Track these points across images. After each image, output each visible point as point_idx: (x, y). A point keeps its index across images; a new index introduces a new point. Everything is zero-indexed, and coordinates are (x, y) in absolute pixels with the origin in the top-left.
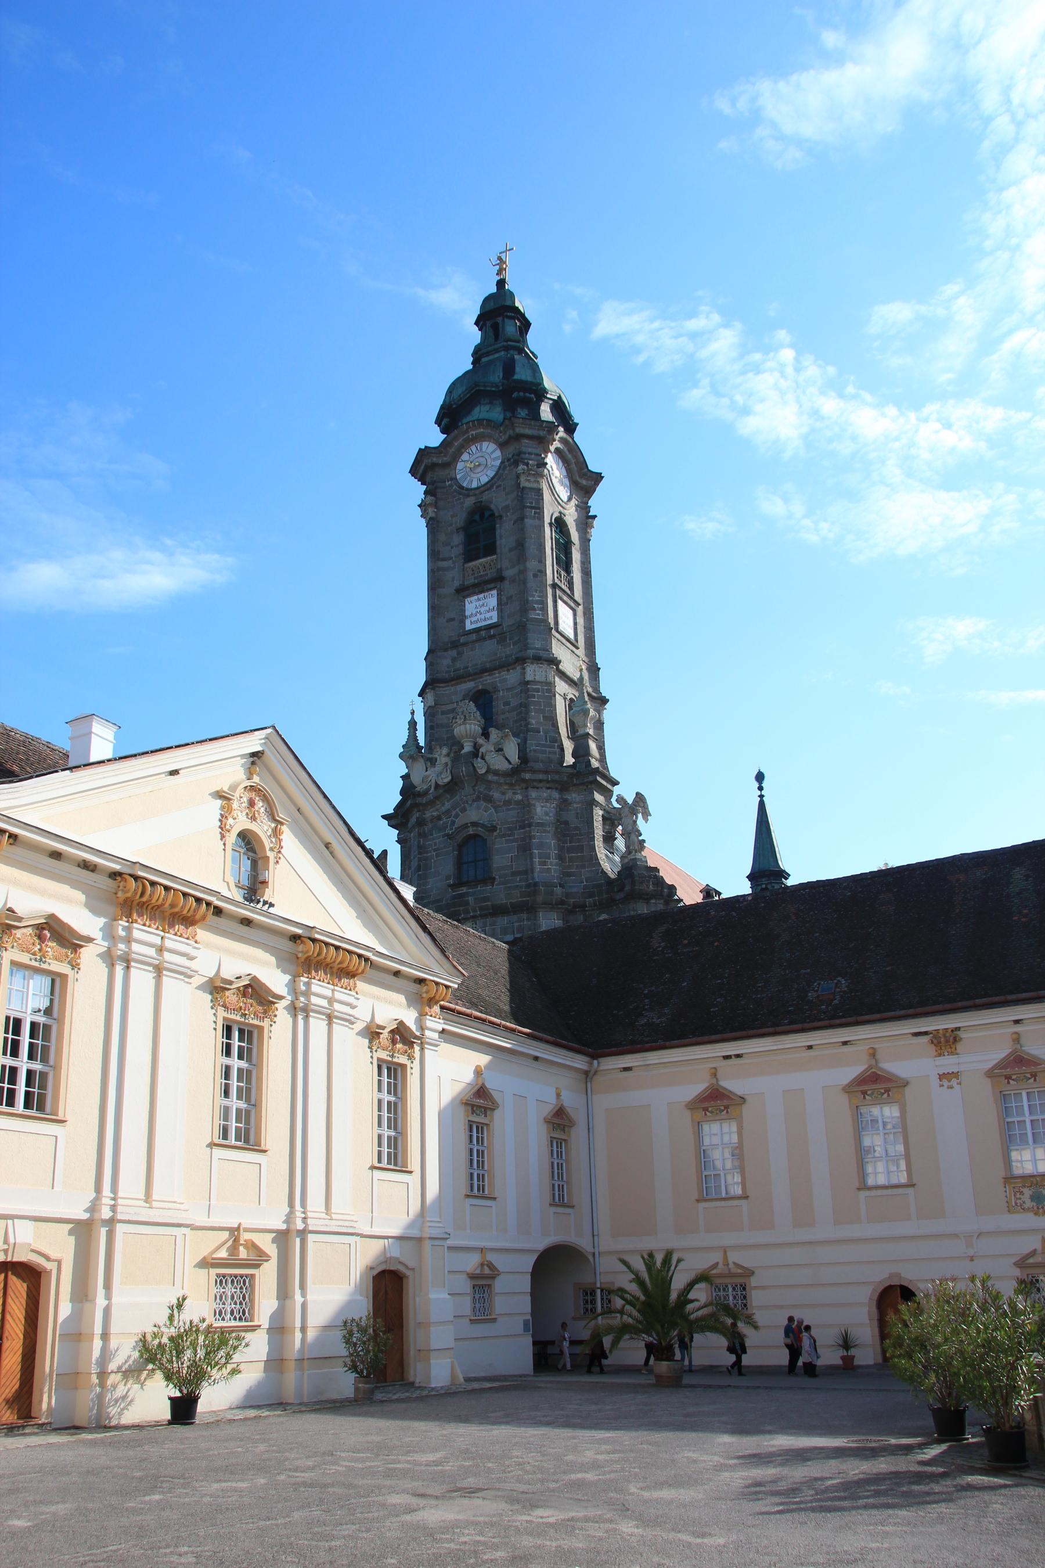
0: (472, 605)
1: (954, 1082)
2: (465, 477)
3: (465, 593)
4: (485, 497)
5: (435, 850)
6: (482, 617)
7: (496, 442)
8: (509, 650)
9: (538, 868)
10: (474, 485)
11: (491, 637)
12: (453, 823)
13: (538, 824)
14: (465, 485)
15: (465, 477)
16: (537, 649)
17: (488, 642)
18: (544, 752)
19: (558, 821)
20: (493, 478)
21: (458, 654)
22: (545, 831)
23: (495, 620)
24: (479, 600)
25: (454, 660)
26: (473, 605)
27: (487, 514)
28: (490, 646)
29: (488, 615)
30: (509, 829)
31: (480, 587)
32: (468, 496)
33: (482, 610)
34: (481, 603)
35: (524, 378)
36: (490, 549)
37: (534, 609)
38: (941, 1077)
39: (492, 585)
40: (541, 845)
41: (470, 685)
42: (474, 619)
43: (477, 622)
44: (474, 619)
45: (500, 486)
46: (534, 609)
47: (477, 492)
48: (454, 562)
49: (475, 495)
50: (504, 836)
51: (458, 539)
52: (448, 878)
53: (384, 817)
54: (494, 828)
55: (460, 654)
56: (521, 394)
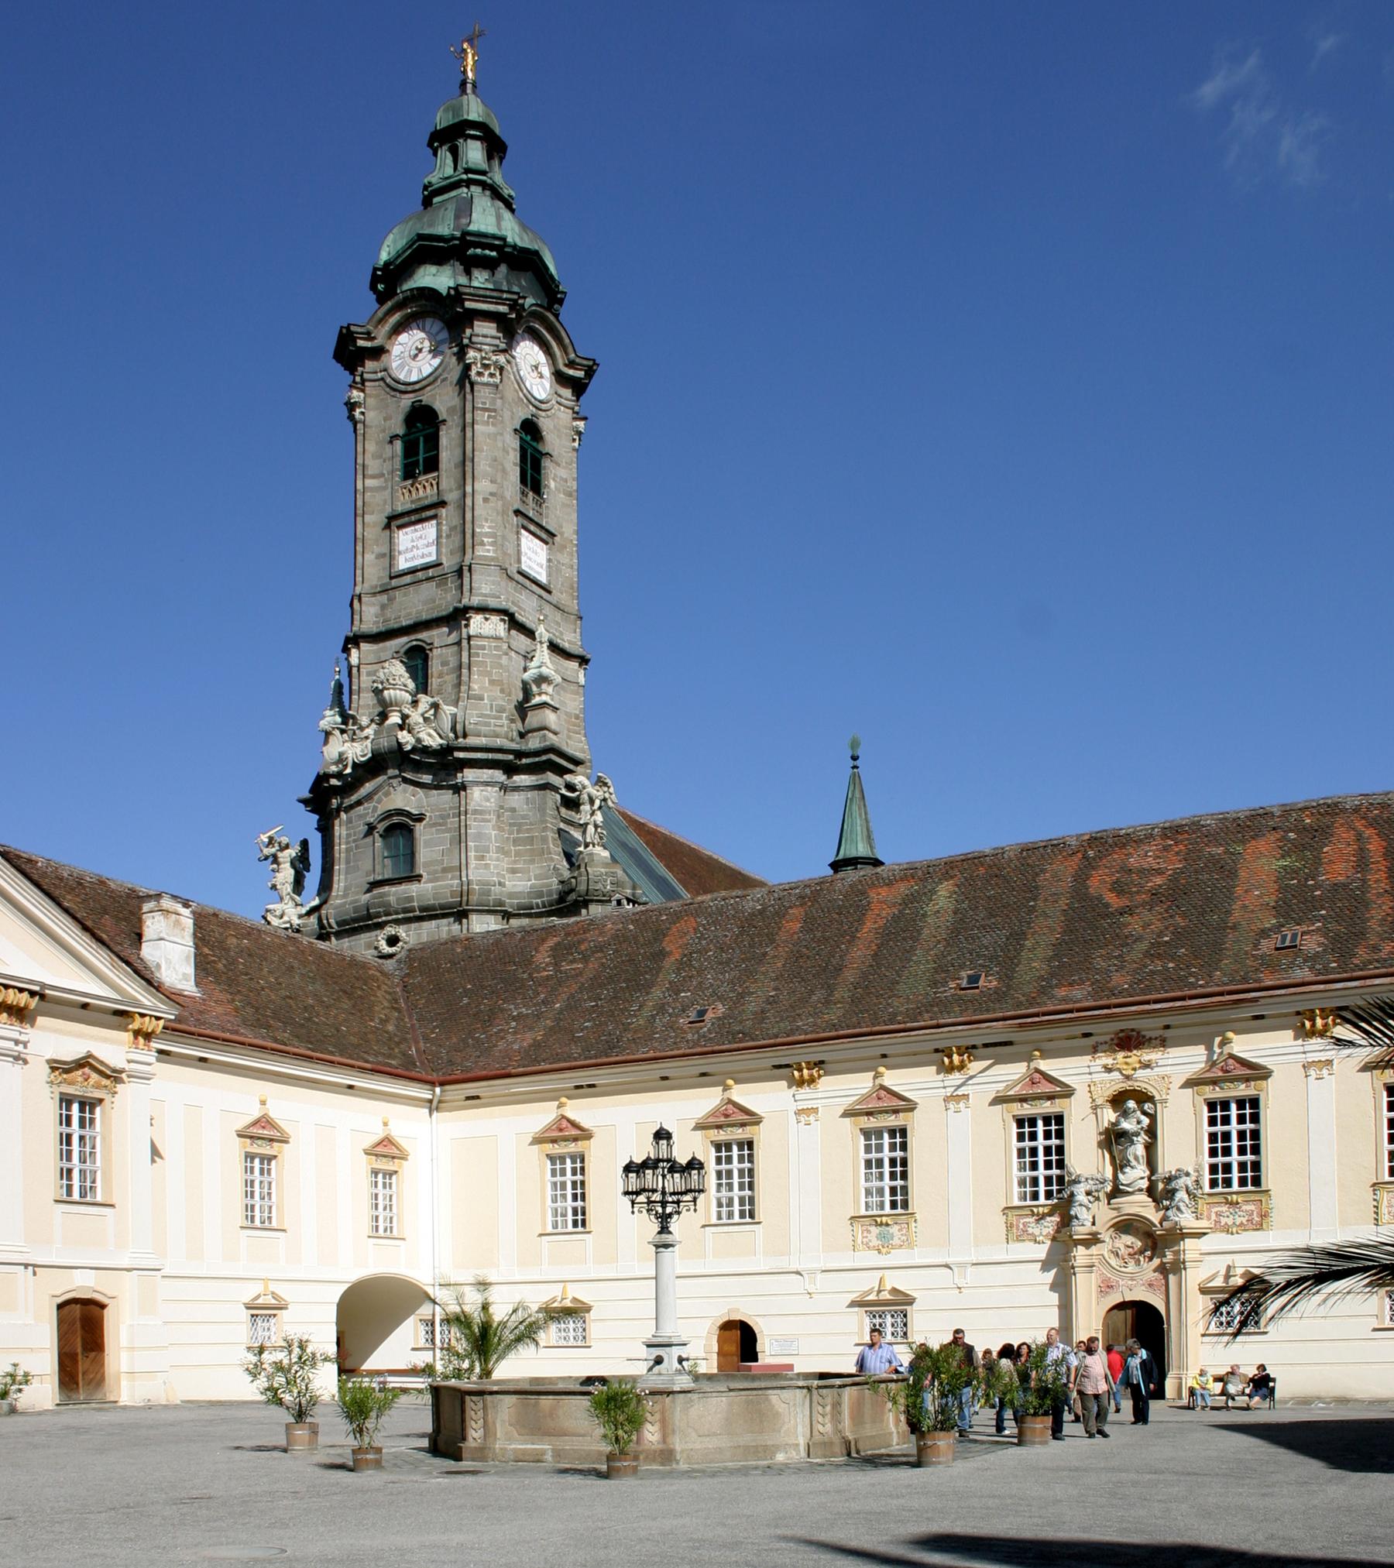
1: (812, 1118)
2: (402, 366)
4: (426, 398)
6: (420, 552)
7: (442, 319)
8: (443, 600)
9: (473, 863)
10: (414, 378)
11: (428, 579)
12: (375, 809)
13: (475, 812)
14: (402, 377)
15: (402, 366)
16: (485, 595)
17: (425, 585)
18: (488, 724)
19: (502, 807)
20: (436, 369)
22: (484, 820)
23: (433, 558)
25: (383, 607)
26: (409, 537)
29: (426, 551)
30: (442, 817)
34: (418, 534)
35: (483, 229)
36: (432, 465)
37: (482, 544)
38: (799, 1113)
40: (479, 836)
41: (404, 639)
42: (409, 555)
43: (412, 559)
44: (409, 555)
46: (482, 544)
50: (435, 825)
53: (300, 801)
54: (420, 818)
55: (391, 600)
56: (479, 251)
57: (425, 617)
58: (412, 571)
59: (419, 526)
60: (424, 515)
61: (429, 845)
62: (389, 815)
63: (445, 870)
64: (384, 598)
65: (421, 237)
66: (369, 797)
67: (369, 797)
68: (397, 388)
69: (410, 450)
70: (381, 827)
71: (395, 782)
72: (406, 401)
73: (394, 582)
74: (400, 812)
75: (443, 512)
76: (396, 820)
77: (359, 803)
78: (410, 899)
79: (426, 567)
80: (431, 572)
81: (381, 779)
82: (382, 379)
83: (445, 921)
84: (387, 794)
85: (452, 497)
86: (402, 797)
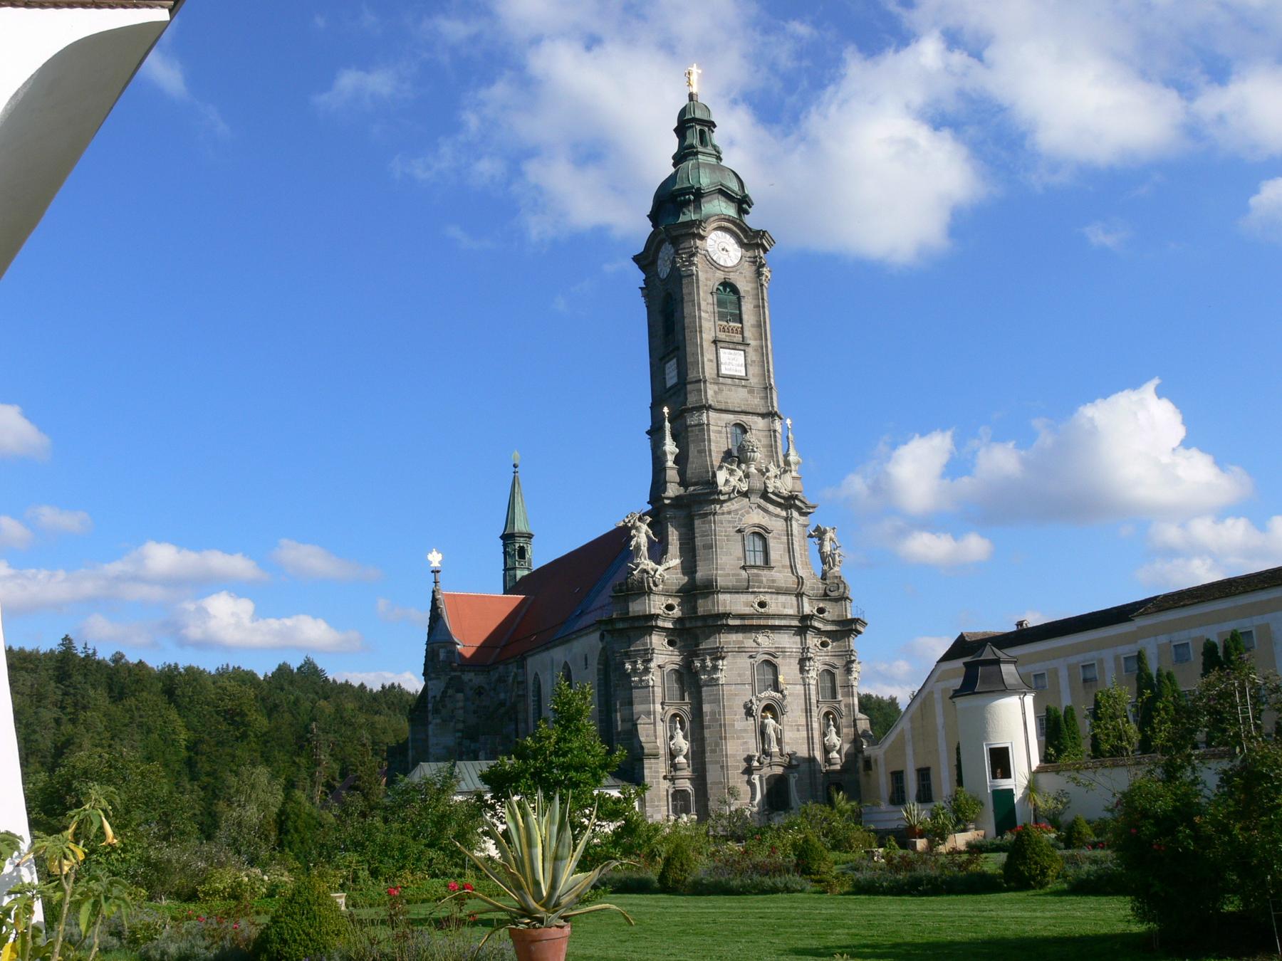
0: (725, 354)
17: (741, 389)
25: (715, 393)
28: (743, 393)
31: (734, 345)
52: (739, 559)
58: (732, 377)
61: (777, 551)
63: (783, 566)
64: (716, 387)
68: (713, 264)
69: (721, 303)
70: (748, 531)
72: (720, 275)
74: (760, 526)
75: (748, 349)
76: (757, 530)
77: (729, 513)
78: (773, 581)
79: (740, 379)
83: (788, 597)
84: (748, 513)
85: (753, 343)
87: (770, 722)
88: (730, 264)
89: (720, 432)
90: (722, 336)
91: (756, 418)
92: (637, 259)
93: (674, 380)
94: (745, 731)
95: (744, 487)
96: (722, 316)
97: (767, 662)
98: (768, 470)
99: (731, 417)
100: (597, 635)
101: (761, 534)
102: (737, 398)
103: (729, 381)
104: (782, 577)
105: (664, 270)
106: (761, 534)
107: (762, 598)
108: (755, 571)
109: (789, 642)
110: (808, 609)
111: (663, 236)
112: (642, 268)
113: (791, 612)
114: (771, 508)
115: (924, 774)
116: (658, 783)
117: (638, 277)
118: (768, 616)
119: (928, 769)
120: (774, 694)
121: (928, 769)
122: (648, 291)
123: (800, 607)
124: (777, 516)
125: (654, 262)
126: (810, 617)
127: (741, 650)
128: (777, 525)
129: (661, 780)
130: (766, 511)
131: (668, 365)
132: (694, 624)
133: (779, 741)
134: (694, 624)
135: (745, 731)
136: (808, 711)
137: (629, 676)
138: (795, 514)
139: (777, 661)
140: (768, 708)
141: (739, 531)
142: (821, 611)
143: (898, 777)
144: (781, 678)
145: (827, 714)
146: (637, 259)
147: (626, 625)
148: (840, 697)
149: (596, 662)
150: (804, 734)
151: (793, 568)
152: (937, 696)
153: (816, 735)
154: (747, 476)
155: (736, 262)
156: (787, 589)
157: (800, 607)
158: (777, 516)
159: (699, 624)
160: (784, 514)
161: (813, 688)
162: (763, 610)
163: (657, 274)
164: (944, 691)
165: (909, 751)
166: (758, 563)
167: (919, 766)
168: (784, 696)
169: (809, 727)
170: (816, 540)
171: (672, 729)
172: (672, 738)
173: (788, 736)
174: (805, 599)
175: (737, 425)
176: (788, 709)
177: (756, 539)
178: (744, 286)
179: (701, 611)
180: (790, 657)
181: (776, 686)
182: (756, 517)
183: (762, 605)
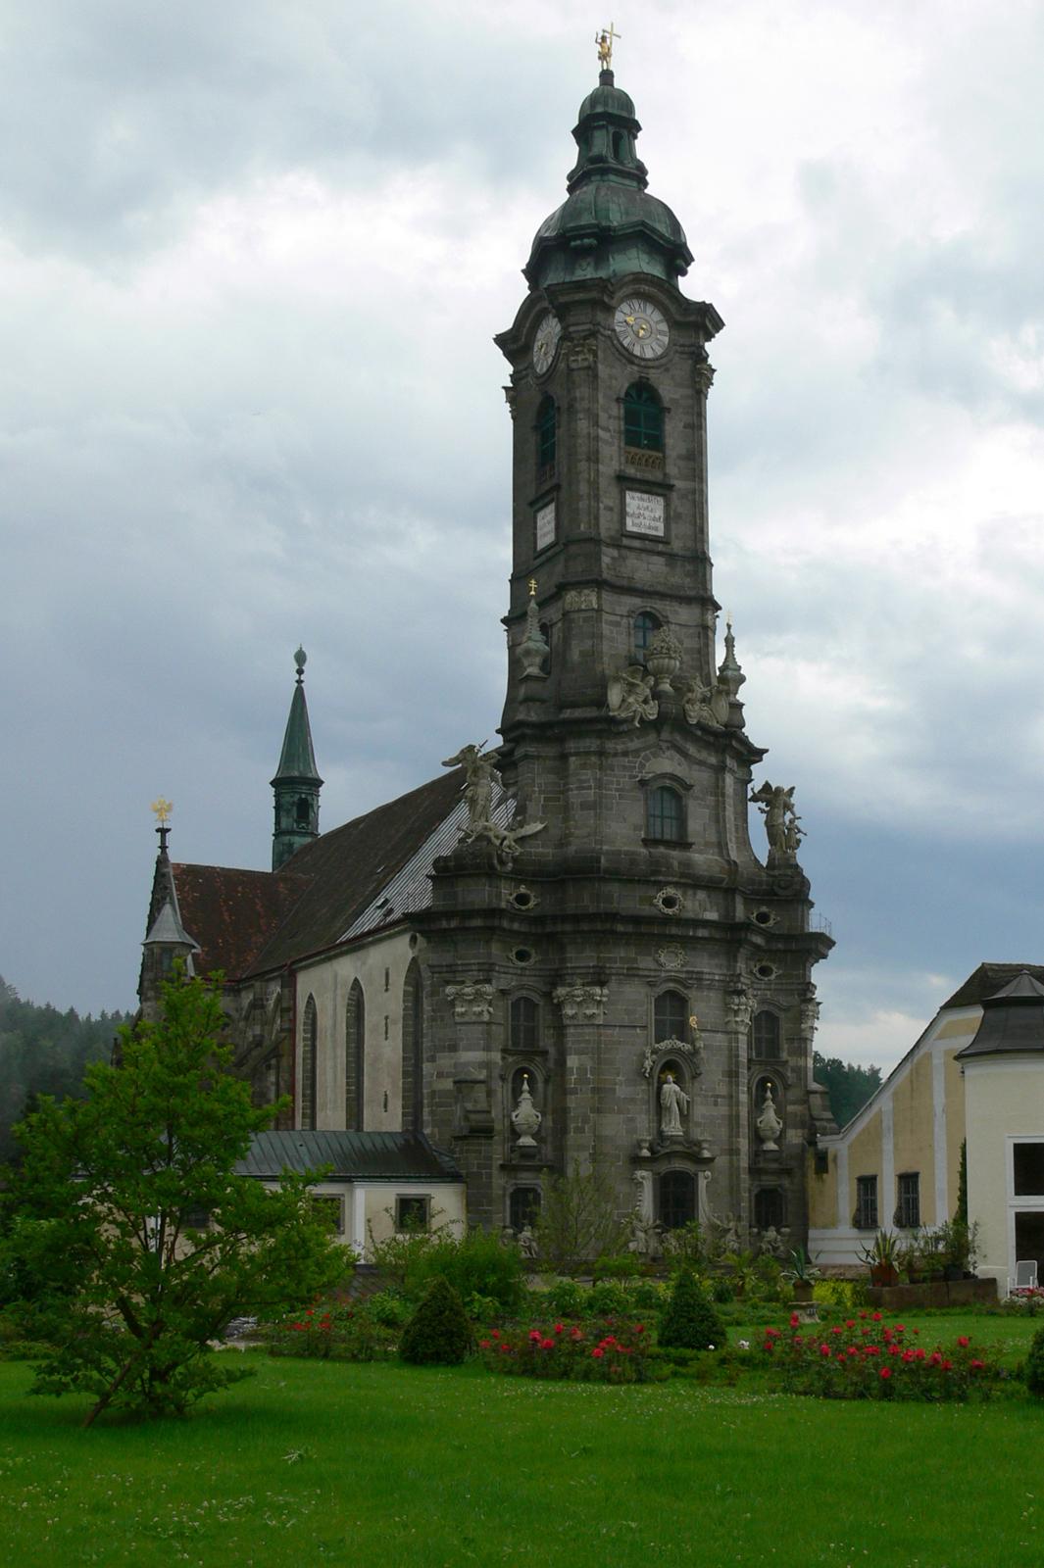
0: (634, 501)
3: (629, 485)
4: (653, 375)
5: (617, 790)
11: (660, 554)
12: (642, 766)
21: (620, 556)
23: (661, 533)
24: (643, 500)
27: (645, 395)
28: (658, 564)
29: (653, 524)
32: (632, 363)
33: (647, 513)
34: (646, 504)
39: (660, 491)
42: (637, 521)
44: (637, 521)
45: (667, 370)
47: (643, 363)
48: (612, 437)
49: (638, 365)
51: (617, 410)
52: (636, 828)
57: (660, 588)
59: (645, 496)
60: (655, 489)
61: (698, 822)
62: (664, 776)
63: (707, 844)
64: (615, 553)
65: (643, 224)
66: (636, 752)
67: (636, 752)
69: (631, 418)
71: (664, 745)
73: (626, 542)
76: (668, 783)
77: (625, 754)
79: (655, 540)
80: (661, 547)
81: (652, 737)
82: (609, 337)
84: (655, 755)
86: (667, 764)
87: (671, 1088)
88: (649, 354)
89: (618, 624)
90: (631, 471)
91: (676, 606)
92: (501, 340)
93: (550, 538)
94: (633, 1100)
95: (652, 711)
96: (631, 438)
97: (671, 994)
98: (691, 690)
99: (636, 602)
100: (407, 938)
101: (674, 791)
102: (647, 570)
103: (637, 544)
104: (703, 859)
105: (542, 359)
106: (674, 791)
107: (670, 891)
108: (662, 849)
109: (709, 966)
110: (740, 913)
111: (546, 304)
112: (510, 355)
113: (712, 915)
114: (692, 750)
115: (908, 1182)
116: (490, 1176)
117: (502, 370)
118: (679, 921)
119: (916, 1176)
120: (680, 1044)
121: (916, 1176)
122: (513, 395)
123: (729, 911)
124: (701, 763)
125: (527, 348)
126: (747, 926)
127: (632, 974)
128: (700, 777)
129: (495, 1172)
130: (684, 754)
131: (540, 515)
132: (559, 928)
133: (685, 1118)
134: (559, 928)
135: (633, 1100)
136: (732, 1075)
137: (452, 1004)
138: (730, 762)
139: (692, 994)
140: (670, 1066)
141: (643, 783)
142: (763, 918)
143: (868, 1185)
144: (693, 1021)
145: (763, 1082)
146: (501, 340)
147: (454, 924)
148: (784, 1056)
149: (402, 980)
150: (723, 1110)
151: (721, 846)
152: (938, 1061)
153: (744, 1112)
154: (656, 695)
155: (659, 351)
156: (711, 880)
157: (729, 911)
158: (701, 763)
159: (568, 927)
160: (713, 760)
161: (743, 1039)
162: (670, 911)
163: (531, 366)
164: (947, 1053)
165: (888, 1146)
166: (667, 837)
167: (903, 1170)
168: (696, 1052)
169: (732, 1099)
170: (763, 805)
171: (516, 1093)
172: (516, 1105)
173: (700, 1111)
174: (739, 900)
175: (646, 615)
176: (702, 1069)
177: (666, 796)
178: (669, 390)
179: (571, 908)
180: (710, 988)
181: (682, 1031)
182: (667, 764)
183: (669, 902)
